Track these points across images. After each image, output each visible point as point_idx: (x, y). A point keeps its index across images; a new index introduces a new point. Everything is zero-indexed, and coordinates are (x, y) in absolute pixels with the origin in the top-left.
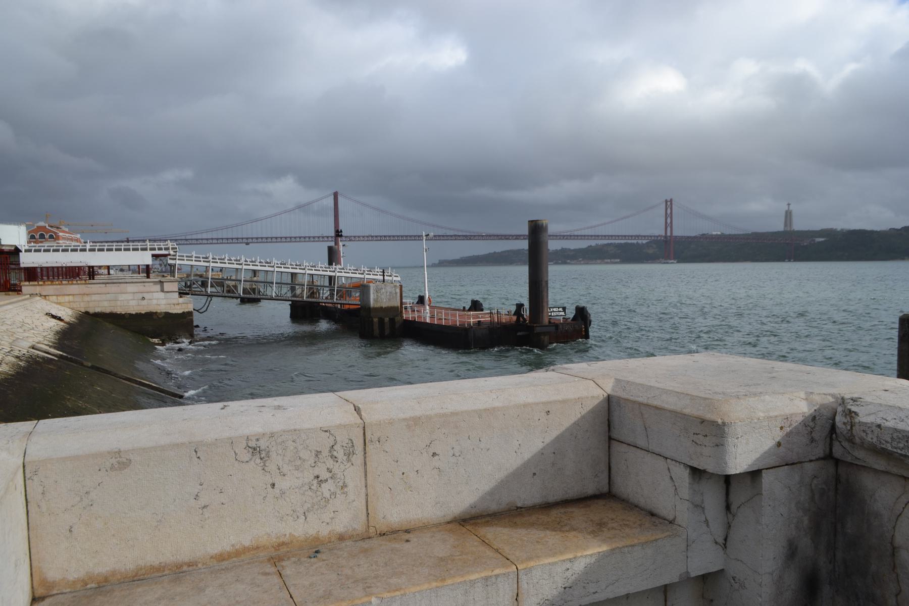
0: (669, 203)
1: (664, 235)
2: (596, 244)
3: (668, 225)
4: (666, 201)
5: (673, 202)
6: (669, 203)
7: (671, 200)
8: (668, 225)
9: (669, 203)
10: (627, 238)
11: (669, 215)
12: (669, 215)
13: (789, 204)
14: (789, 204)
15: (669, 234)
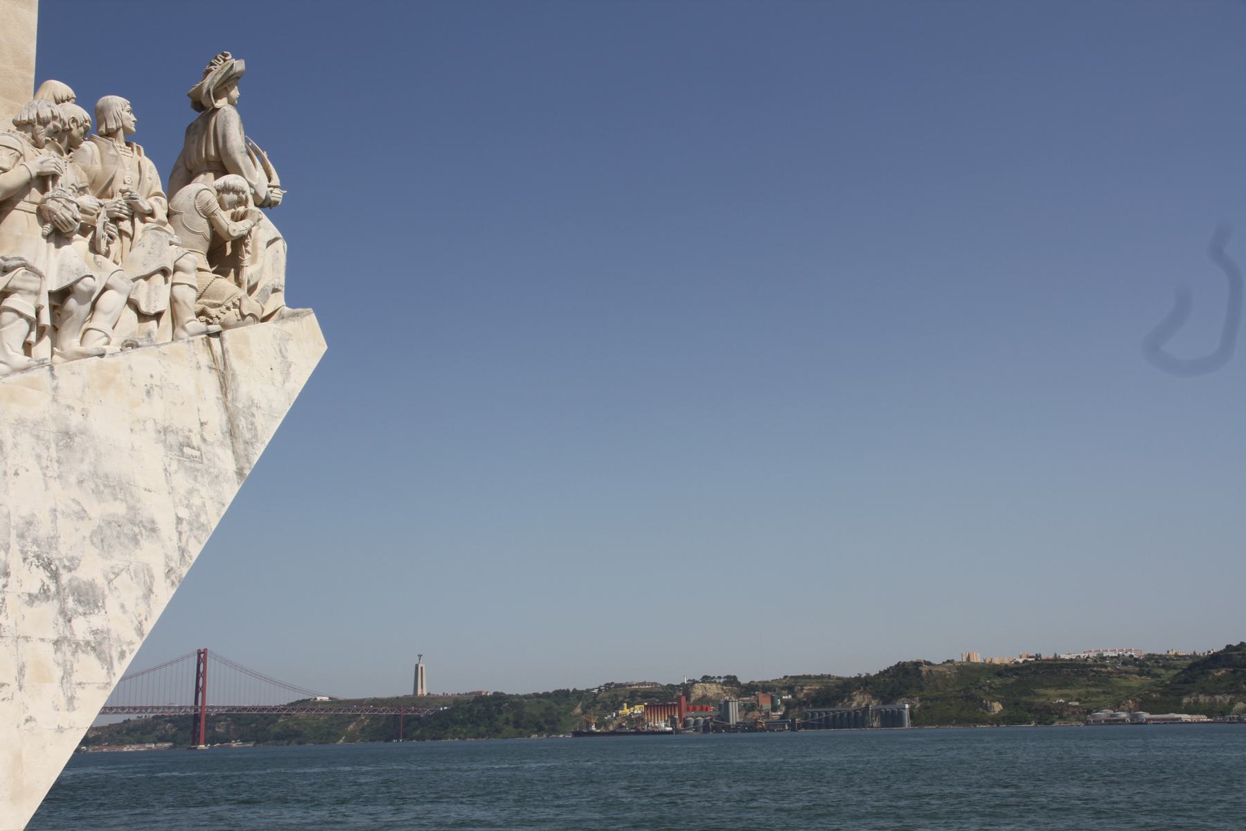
0: (202, 656)
1: (193, 704)
2: (129, 719)
3: (199, 689)
4: (199, 654)
5: (208, 654)
6: (202, 656)
7: (205, 652)
8: (199, 689)
9: (202, 655)
10: (149, 711)
11: (201, 675)
12: (201, 675)
13: (420, 656)
14: (420, 656)
15: (200, 704)
